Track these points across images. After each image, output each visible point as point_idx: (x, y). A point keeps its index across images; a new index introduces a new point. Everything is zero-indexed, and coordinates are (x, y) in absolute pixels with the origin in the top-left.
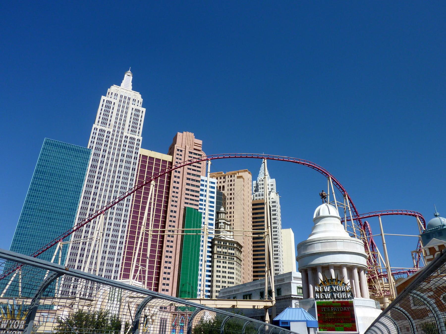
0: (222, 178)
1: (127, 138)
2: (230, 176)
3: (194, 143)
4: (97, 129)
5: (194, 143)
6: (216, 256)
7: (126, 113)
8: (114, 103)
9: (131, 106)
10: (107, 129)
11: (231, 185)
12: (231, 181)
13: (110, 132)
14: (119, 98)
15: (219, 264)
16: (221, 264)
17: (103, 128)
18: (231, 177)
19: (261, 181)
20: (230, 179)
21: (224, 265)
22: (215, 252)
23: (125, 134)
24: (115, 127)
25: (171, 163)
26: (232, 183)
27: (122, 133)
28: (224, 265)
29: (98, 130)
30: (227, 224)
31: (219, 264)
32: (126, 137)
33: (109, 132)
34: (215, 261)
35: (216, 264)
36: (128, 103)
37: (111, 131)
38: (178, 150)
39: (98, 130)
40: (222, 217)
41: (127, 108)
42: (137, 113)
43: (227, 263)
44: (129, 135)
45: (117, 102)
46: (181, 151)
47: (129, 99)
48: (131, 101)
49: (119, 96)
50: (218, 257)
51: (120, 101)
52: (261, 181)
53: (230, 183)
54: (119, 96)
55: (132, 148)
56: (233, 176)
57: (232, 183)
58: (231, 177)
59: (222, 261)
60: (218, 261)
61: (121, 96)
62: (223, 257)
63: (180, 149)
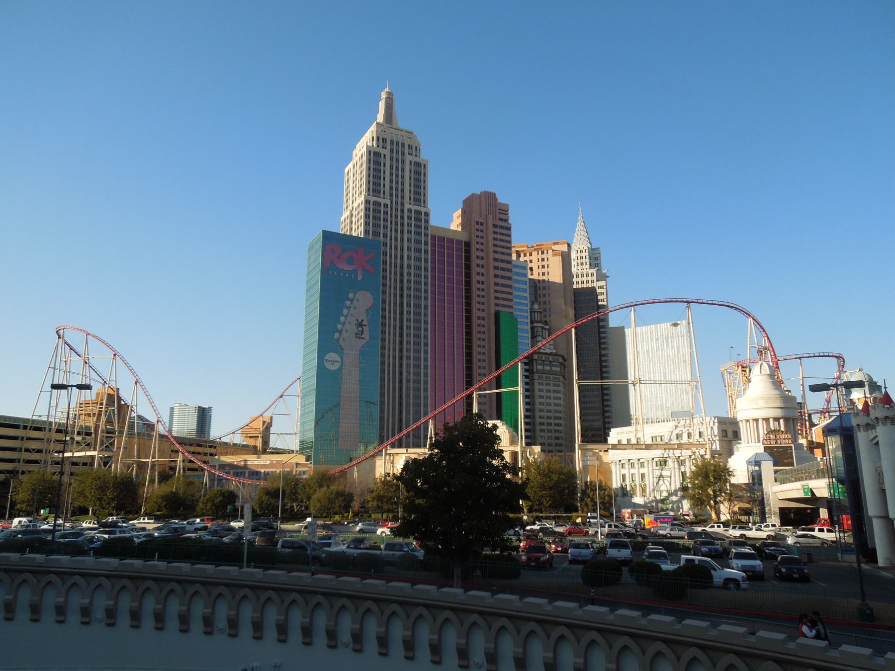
0: (528, 254)
1: (411, 212)
2: (540, 252)
3: (499, 209)
4: (370, 201)
5: (499, 209)
6: (536, 376)
7: (403, 170)
8: (385, 155)
9: (408, 158)
10: (383, 201)
11: (543, 267)
12: (543, 260)
13: (387, 205)
14: (388, 146)
15: (541, 387)
16: (544, 387)
17: (378, 199)
18: (543, 253)
19: (579, 252)
20: (540, 256)
21: (548, 388)
22: (535, 371)
23: (407, 206)
24: (391, 195)
25: (468, 244)
26: (545, 263)
27: (402, 204)
28: (548, 388)
29: (372, 203)
30: (545, 329)
31: (541, 387)
32: (410, 211)
33: (386, 206)
34: (536, 382)
35: (537, 387)
36: (403, 154)
37: (389, 202)
38: (477, 223)
39: (372, 203)
40: (536, 319)
41: (403, 162)
42: (418, 169)
43: (544, 384)
44: (414, 208)
45: (387, 152)
46: (482, 224)
47: (403, 145)
48: (406, 150)
49: (388, 142)
50: (539, 377)
51: (392, 151)
52: (579, 252)
53: (540, 264)
54: (388, 142)
55: (420, 227)
56: (545, 252)
57: (545, 263)
58: (543, 253)
59: (544, 382)
60: (539, 384)
61: (392, 142)
62: (546, 377)
63: (480, 220)
